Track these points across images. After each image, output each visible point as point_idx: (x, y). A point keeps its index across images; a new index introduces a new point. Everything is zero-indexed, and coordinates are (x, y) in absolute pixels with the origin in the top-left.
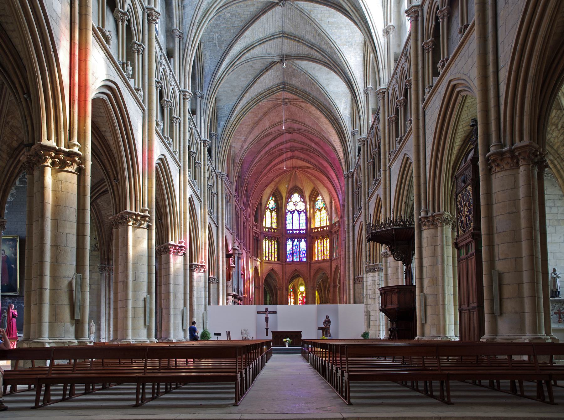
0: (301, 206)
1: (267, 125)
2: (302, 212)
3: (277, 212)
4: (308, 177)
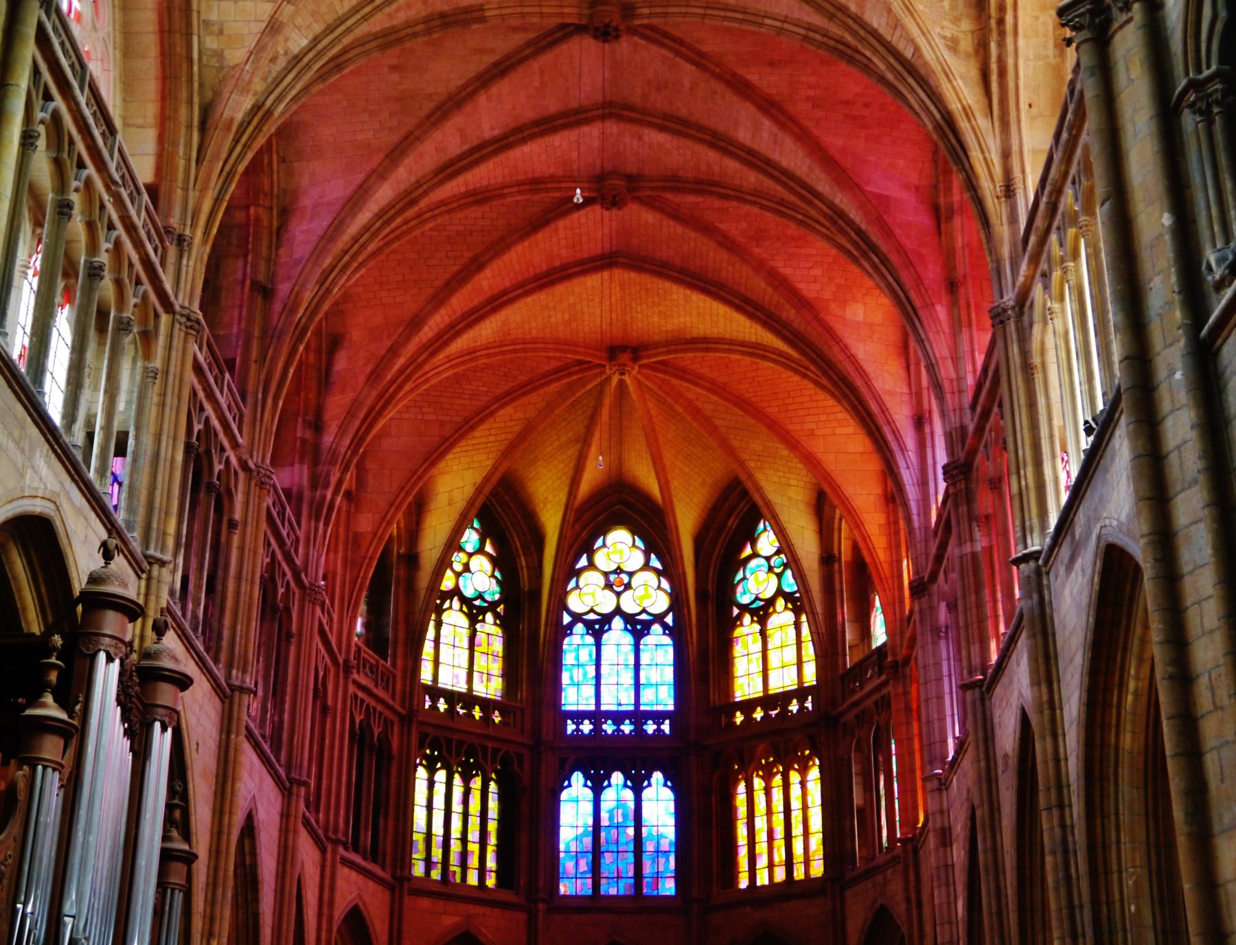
2: (656, 628)
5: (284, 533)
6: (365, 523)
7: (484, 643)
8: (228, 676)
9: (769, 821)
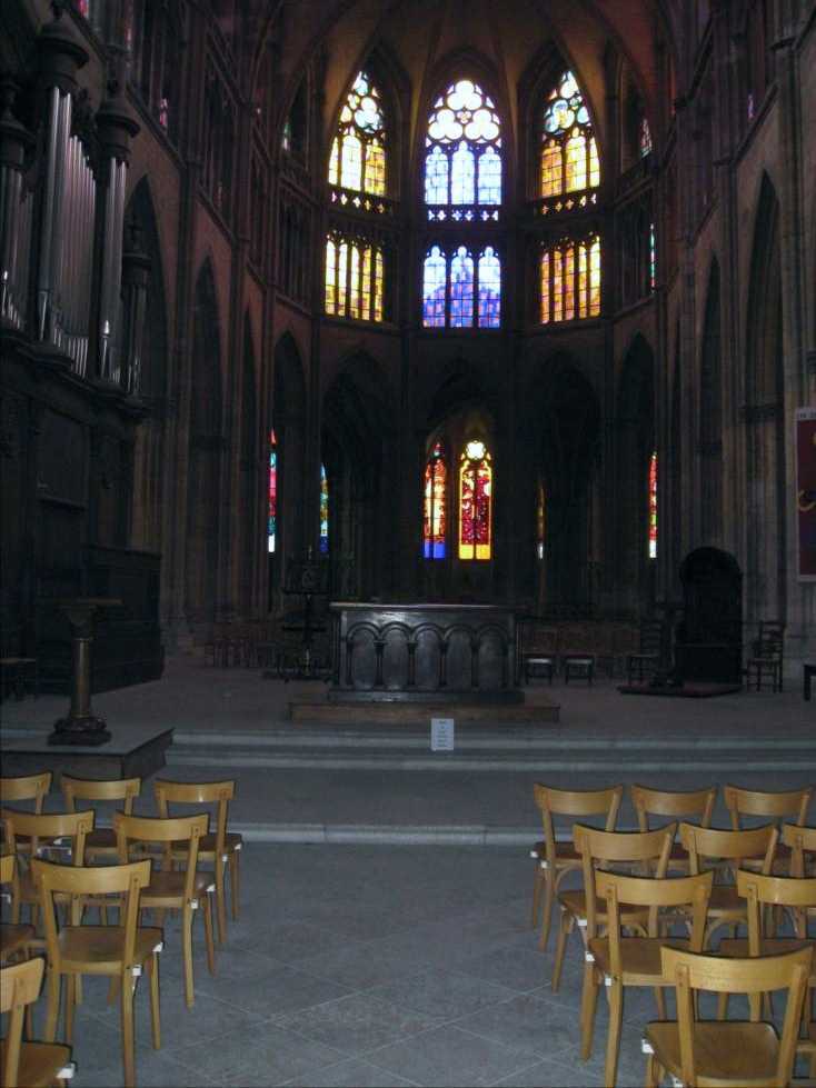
0: (486, 126)
2: (490, 149)
3: (385, 145)
5: (225, 60)
6: (287, 67)
7: (372, 158)
8: (185, 156)
9: (564, 280)
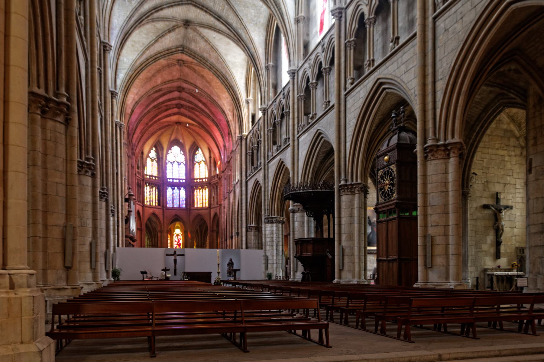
0: (181, 158)
1: (159, 81)
4: (190, 133)
